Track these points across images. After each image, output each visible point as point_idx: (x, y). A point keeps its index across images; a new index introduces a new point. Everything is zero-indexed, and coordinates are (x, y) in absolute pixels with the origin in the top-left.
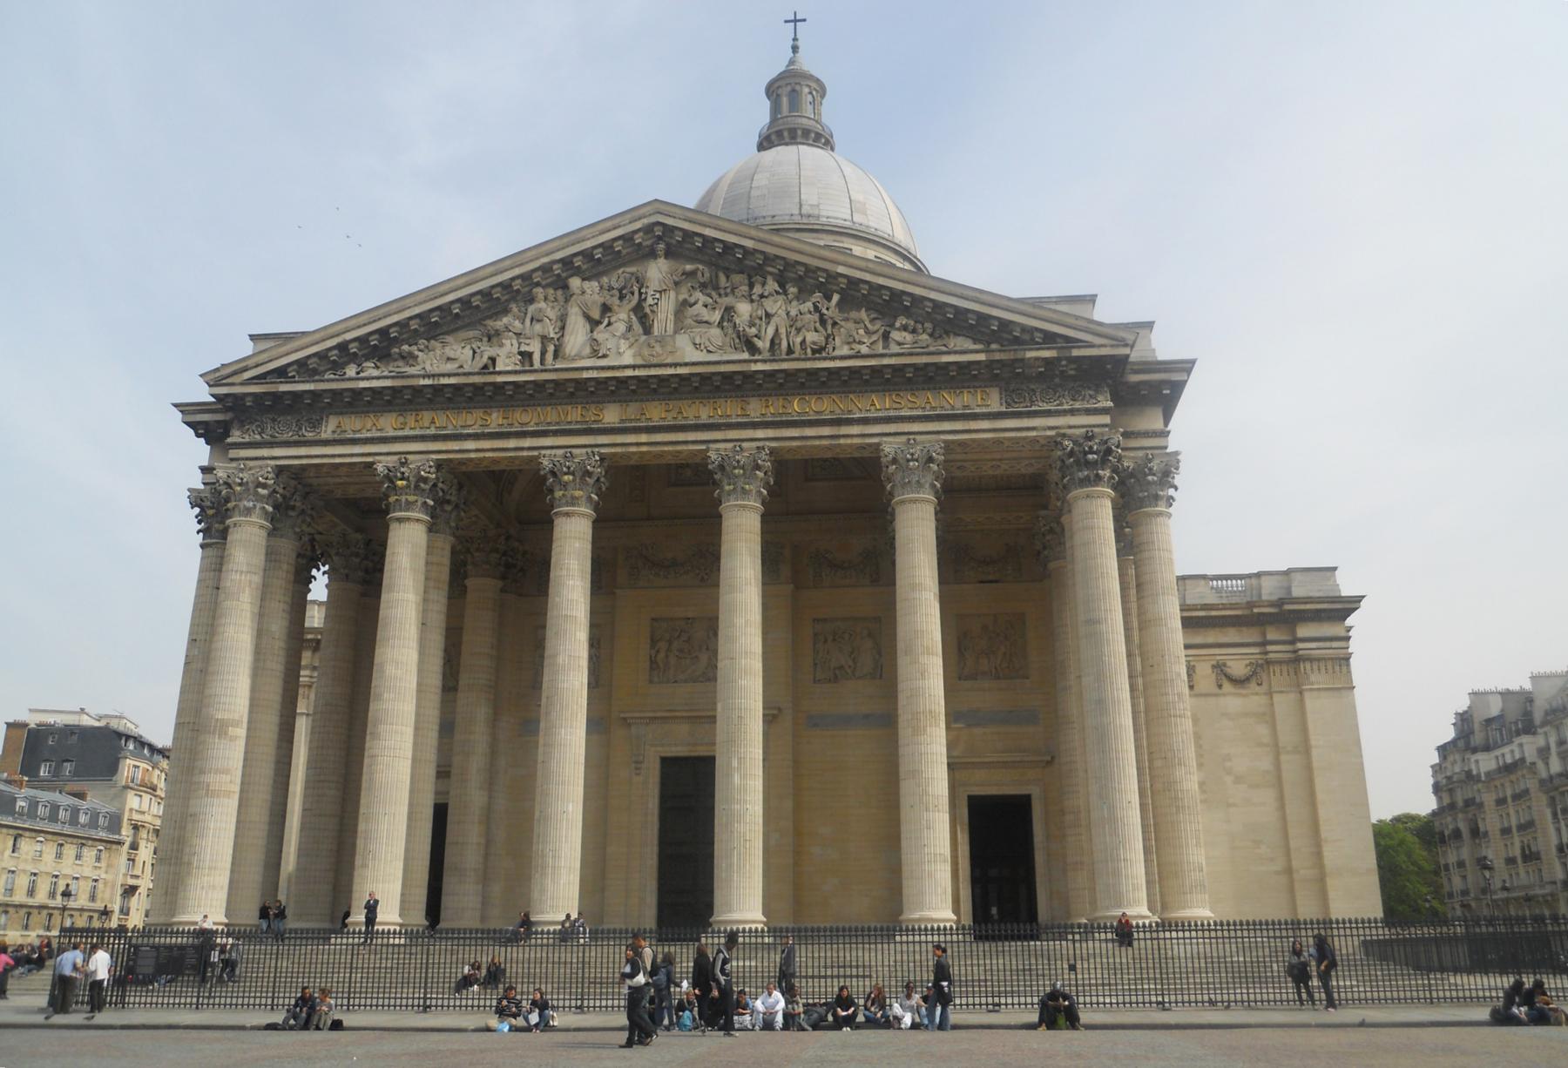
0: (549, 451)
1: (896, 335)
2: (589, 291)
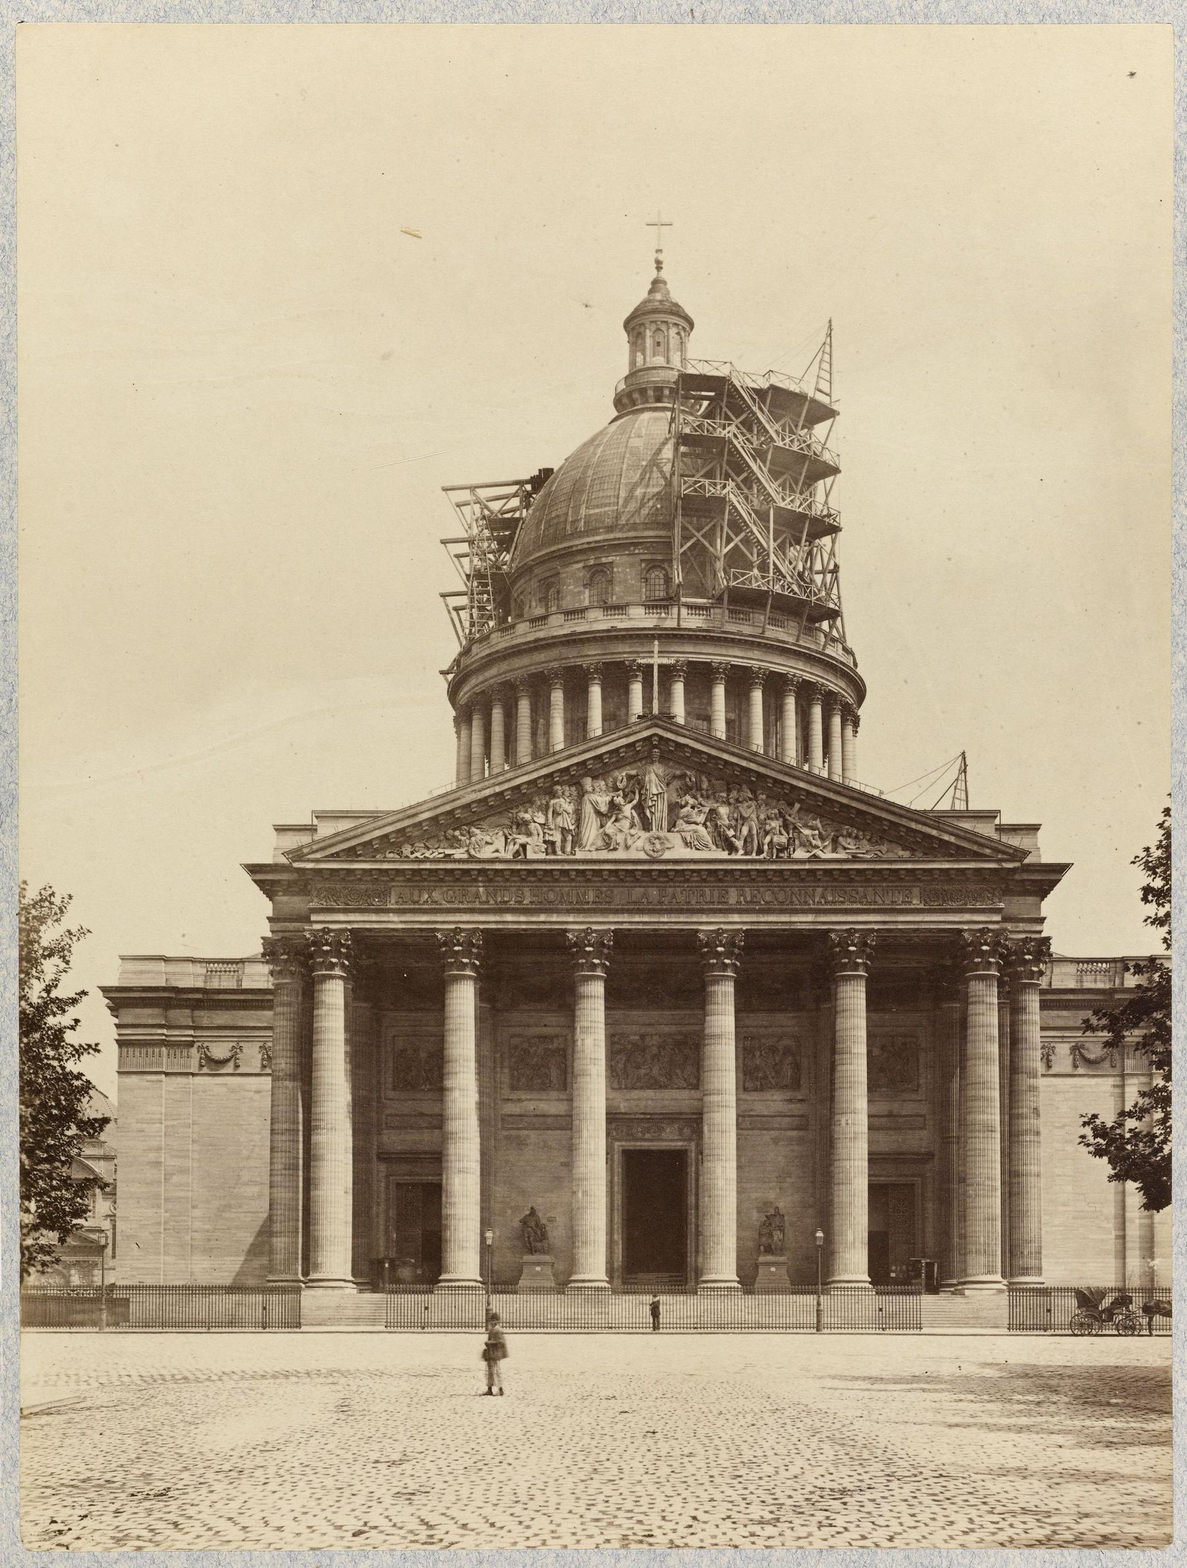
1: (841, 839)
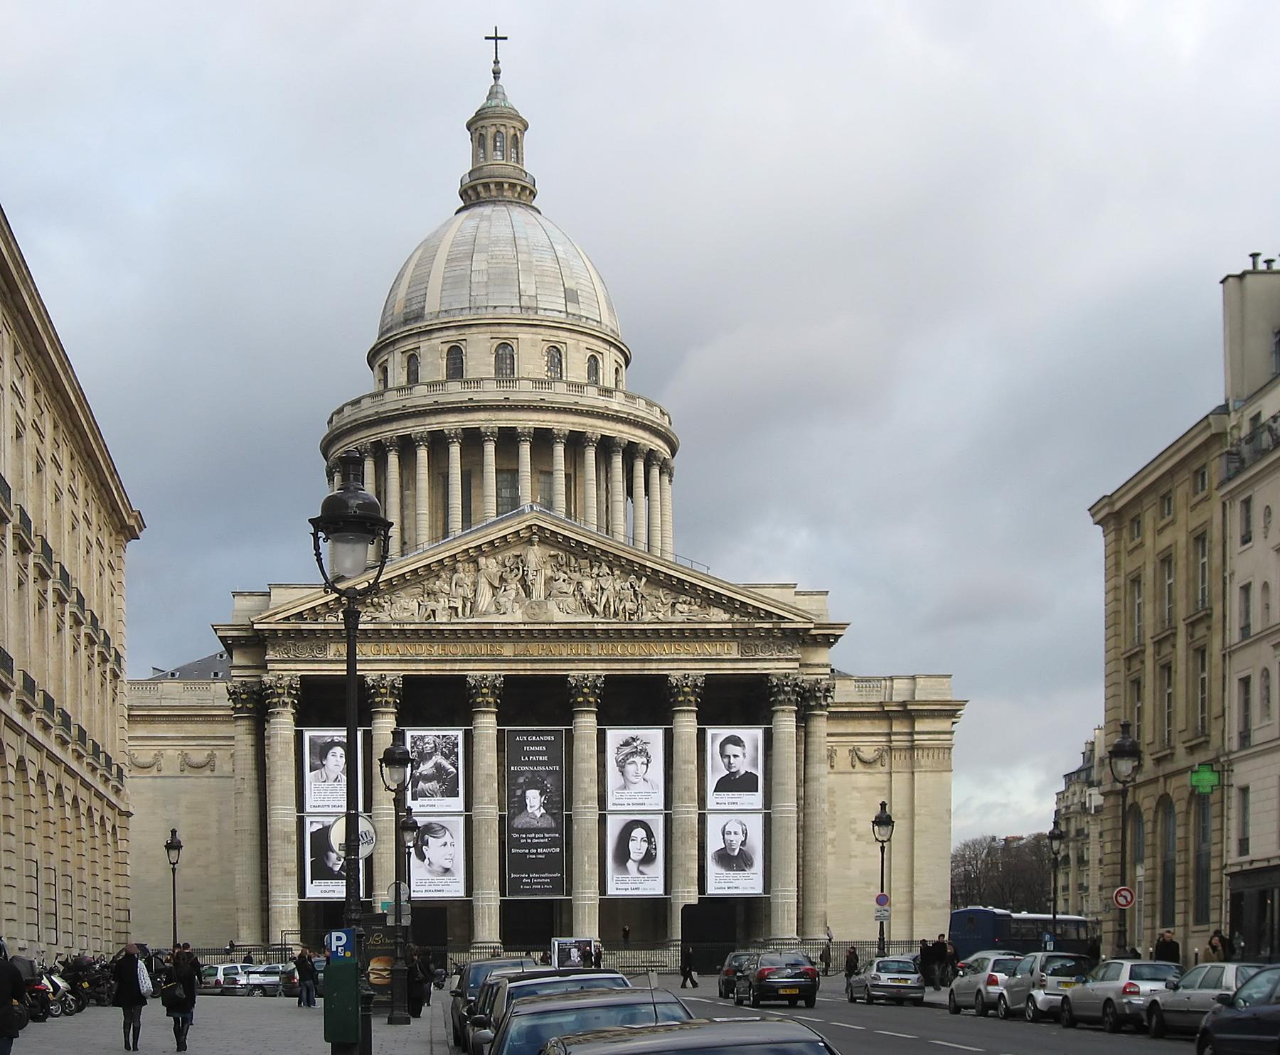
0: (473, 672)
1: (678, 606)
2: (490, 565)
